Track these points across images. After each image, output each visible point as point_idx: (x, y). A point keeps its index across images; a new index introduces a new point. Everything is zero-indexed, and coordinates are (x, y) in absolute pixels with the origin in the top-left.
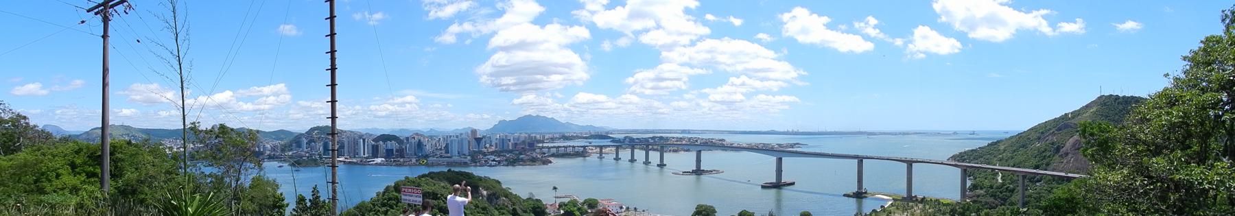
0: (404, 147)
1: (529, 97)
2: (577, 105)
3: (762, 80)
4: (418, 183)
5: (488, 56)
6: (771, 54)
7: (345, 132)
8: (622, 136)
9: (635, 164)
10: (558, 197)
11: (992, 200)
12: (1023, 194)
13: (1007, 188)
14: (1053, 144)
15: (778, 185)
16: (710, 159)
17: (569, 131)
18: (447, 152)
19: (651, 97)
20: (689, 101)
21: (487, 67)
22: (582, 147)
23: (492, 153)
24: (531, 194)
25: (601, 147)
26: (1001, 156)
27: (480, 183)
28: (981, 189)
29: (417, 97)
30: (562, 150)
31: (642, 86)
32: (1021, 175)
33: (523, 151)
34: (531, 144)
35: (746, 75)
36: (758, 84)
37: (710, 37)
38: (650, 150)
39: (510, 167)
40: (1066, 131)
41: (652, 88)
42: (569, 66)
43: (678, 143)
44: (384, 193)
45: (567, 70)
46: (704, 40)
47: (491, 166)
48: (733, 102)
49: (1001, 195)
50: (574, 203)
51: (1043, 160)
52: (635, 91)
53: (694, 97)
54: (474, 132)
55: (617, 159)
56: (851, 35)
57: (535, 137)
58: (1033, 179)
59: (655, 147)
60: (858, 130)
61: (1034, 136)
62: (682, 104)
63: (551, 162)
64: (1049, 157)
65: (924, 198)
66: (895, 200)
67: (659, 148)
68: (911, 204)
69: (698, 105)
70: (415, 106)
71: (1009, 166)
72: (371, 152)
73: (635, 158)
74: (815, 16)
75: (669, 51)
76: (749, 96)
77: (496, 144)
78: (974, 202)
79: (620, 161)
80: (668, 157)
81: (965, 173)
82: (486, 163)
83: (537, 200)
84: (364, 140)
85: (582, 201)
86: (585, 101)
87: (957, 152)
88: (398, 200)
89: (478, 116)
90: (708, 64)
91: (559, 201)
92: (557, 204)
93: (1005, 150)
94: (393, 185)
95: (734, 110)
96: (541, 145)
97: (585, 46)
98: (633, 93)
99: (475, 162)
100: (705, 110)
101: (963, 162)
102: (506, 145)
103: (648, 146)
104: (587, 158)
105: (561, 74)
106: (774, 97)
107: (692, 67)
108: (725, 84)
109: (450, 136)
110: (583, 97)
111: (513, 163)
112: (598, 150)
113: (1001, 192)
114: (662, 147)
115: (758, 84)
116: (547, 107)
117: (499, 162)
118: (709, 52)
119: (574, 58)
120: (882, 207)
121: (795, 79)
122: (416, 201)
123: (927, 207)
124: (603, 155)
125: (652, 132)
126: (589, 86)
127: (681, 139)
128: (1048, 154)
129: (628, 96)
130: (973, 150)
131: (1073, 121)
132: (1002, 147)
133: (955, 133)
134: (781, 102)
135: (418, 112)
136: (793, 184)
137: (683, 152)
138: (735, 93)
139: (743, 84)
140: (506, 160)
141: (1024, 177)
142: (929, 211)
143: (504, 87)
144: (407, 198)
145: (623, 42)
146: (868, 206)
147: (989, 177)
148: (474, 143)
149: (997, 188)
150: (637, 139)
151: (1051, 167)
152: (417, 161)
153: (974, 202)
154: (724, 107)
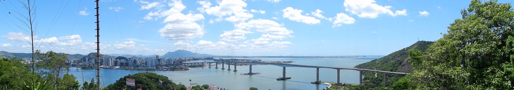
0: (128, 62)
1: (180, 42)
2: (200, 46)
3: (275, 35)
4: (134, 77)
5: (163, 25)
6: (277, 24)
7: (104, 55)
8: (218, 59)
9: (224, 70)
10: (191, 84)
11: (373, 84)
12: (386, 82)
13: (379, 79)
14: (398, 61)
15: (284, 79)
16: (255, 68)
17: (196, 56)
18: (146, 65)
19: (231, 42)
20: (246, 44)
21: (162, 30)
22: (202, 63)
23: (165, 65)
24: (180, 83)
25: (210, 63)
26: (376, 66)
27: (159, 78)
28: (368, 79)
29: (134, 41)
31: (227, 38)
32: (385, 74)
33: (177, 65)
34: (181, 62)
35: (269, 33)
36: (274, 37)
37: (254, 18)
38: (231, 64)
39: (172, 72)
40: (404, 55)
41: (231, 39)
42: (195, 30)
44: (119, 81)
45: (194, 31)
46: (251, 20)
47: (164, 71)
48: (264, 44)
49: (376, 82)
50: (198, 86)
51: (394, 68)
52: (224, 40)
53: (248, 43)
54: (157, 56)
55: (217, 68)
56: (311, 17)
57: (182, 59)
58: (390, 76)
59: (233, 63)
60: (317, 56)
61: (391, 58)
62: (243, 45)
63: (189, 69)
64: (397, 66)
65: (345, 84)
66: (332, 84)
67: (234, 64)
68: (339, 86)
69: (250, 46)
70: (133, 45)
71: (380, 70)
72: (114, 64)
74: (296, 10)
75: (237, 24)
76: (270, 42)
77: (166, 62)
78: (365, 85)
80: (238, 67)
81: (362, 73)
82: (162, 70)
83: (183, 85)
84: (111, 59)
85: (201, 86)
86: (203, 44)
87: (358, 64)
88: (125, 84)
89: (159, 50)
90: (253, 29)
91: (192, 86)
92: (191, 87)
93: (378, 64)
94: (123, 77)
95: (264, 47)
96: (184, 62)
97: (203, 22)
98: (223, 41)
99: (157, 69)
100: (253, 48)
101: (360, 68)
102: (170, 62)
103: (229, 63)
104: (204, 68)
105: (192, 33)
106: (281, 42)
107: (247, 31)
108: (260, 37)
109: (148, 58)
110: (202, 42)
111: (173, 69)
112: (209, 64)
113: (377, 81)
114: (235, 63)
115: (274, 37)
116: (187, 47)
117: (167, 69)
118: (254, 24)
119: (198, 26)
120: (327, 88)
121: (289, 34)
122: (132, 85)
123: (346, 88)
124: (211, 66)
125: (231, 57)
126: (204, 38)
128: (396, 65)
129: (221, 42)
130: (364, 63)
131: (407, 51)
132: (377, 62)
133: (357, 56)
134: (284, 44)
135: (134, 48)
136: (290, 78)
137: (244, 66)
138: (264, 41)
139: (268, 37)
140: (170, 68)
141: (386, 75)
142: (347, 89)
143: (171, 38)
144: (129, 83)
145: (218, 20)
146: (321, 87)
147: (372, 75)
148: (158, 61)
149: (375, 79)
150: (225, 60)
151: (398, 70)
152: (134, 68)
153: (365, 85)
154: (260, 47)
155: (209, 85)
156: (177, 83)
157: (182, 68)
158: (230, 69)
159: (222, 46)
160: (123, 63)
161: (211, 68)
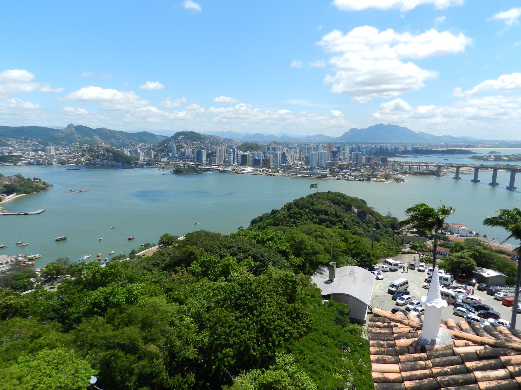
25: (458, 168)
39: (365, 183)
47: (348, 180)
55: (475, 181)
63: (403, 180)
73: (497, 182)
79: (478, 184)
104: (440, 178)
112: (455, 169)
124: (460, 176)
140: (361, 176)
155: (450, 224)
156: (384, 214)
157: (388, 175)
160: (259, 160)
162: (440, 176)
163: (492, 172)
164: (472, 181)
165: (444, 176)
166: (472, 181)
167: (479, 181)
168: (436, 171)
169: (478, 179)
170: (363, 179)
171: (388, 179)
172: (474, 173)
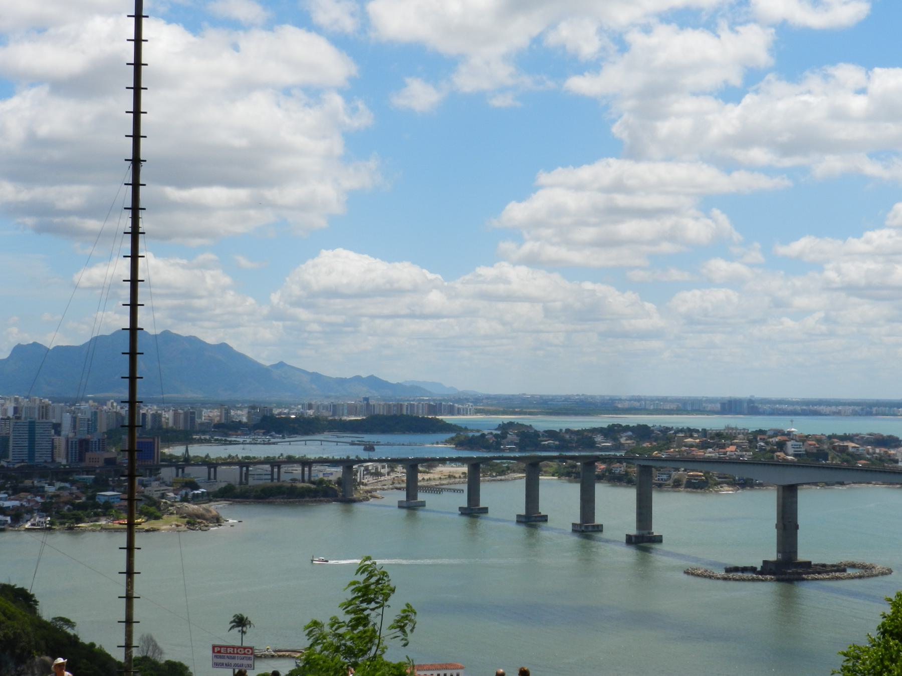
25: (412, 466)
30: (260, 476)
38: (600, 478)
43: (710, 453)
63: (217, 521)
67: (634, 470)
73: (543, 510)
79: (483, 523)
96: (177, 451)
98: (532, 261)
103: (590, 463)
104: (357, 506)
112: (400, 472)
114: (646, 471)
124: (421, 497)
127: (718, 438)
137: (727, 490)
150: (551, 434)
158: (598, 521)
159: (523, 308)
161: (421, 514)
162: (354, 501)
163: (524, 481)
164: (464, 512)
165: (367, 500)
166: (464, 512)
167: (485, 510)
168: (339, 482)
169: (482, 505)
170: (51, 523)
171: (157, 518)
172: (465, 487)
